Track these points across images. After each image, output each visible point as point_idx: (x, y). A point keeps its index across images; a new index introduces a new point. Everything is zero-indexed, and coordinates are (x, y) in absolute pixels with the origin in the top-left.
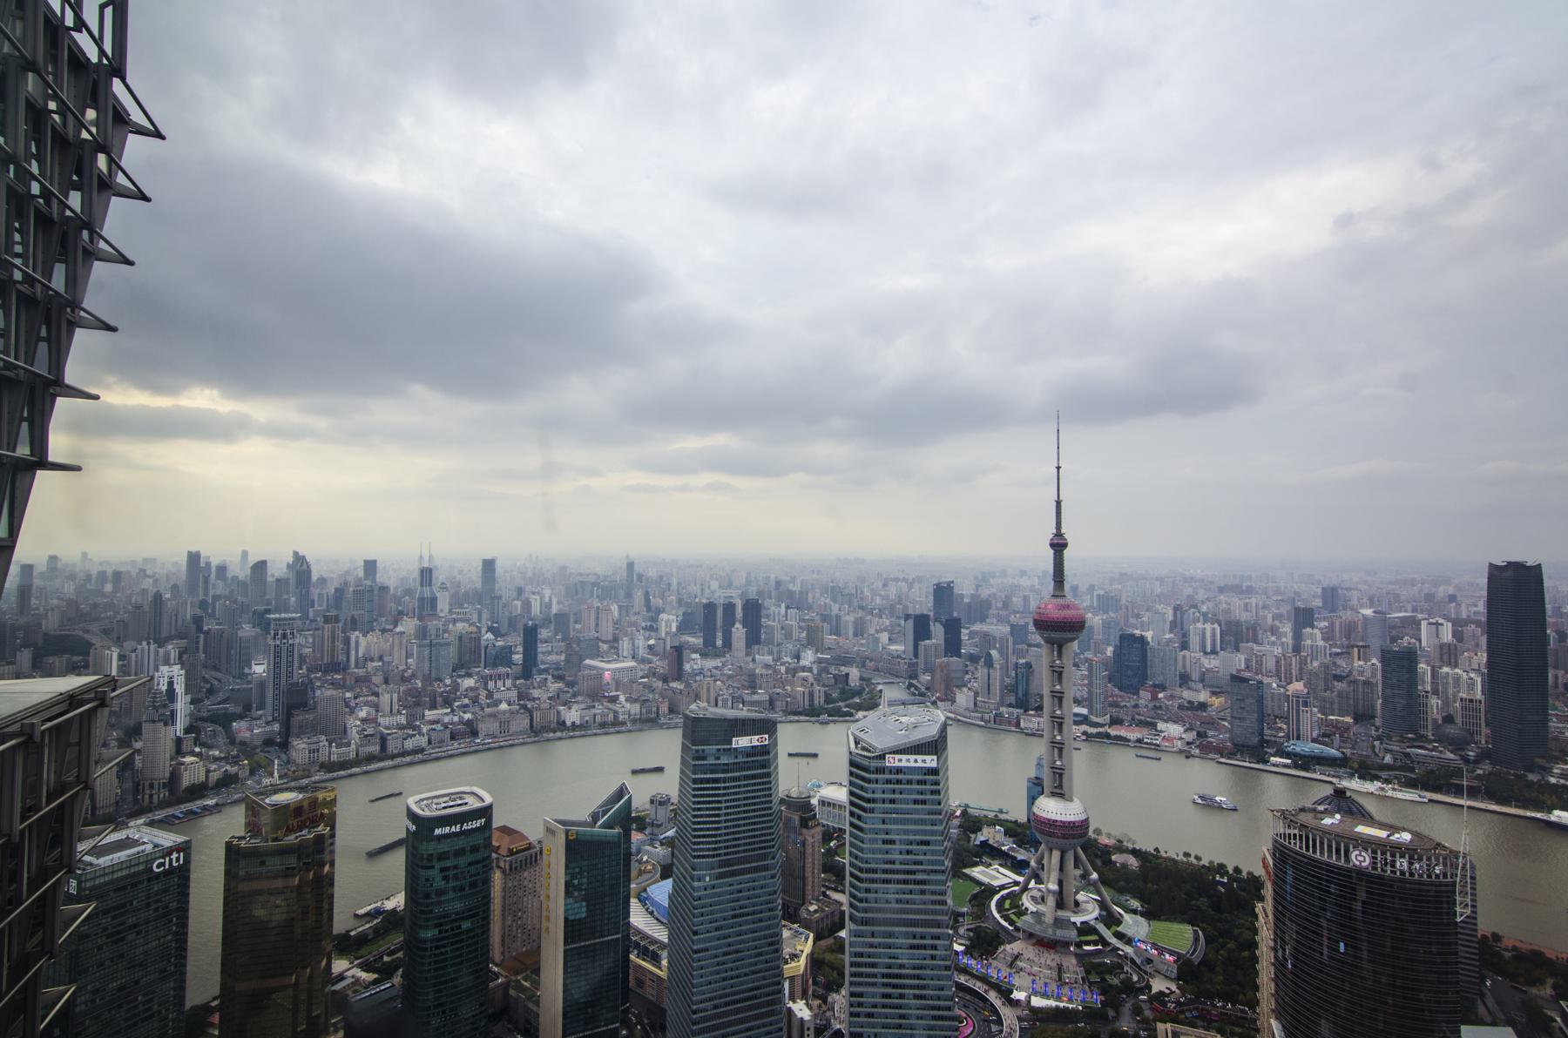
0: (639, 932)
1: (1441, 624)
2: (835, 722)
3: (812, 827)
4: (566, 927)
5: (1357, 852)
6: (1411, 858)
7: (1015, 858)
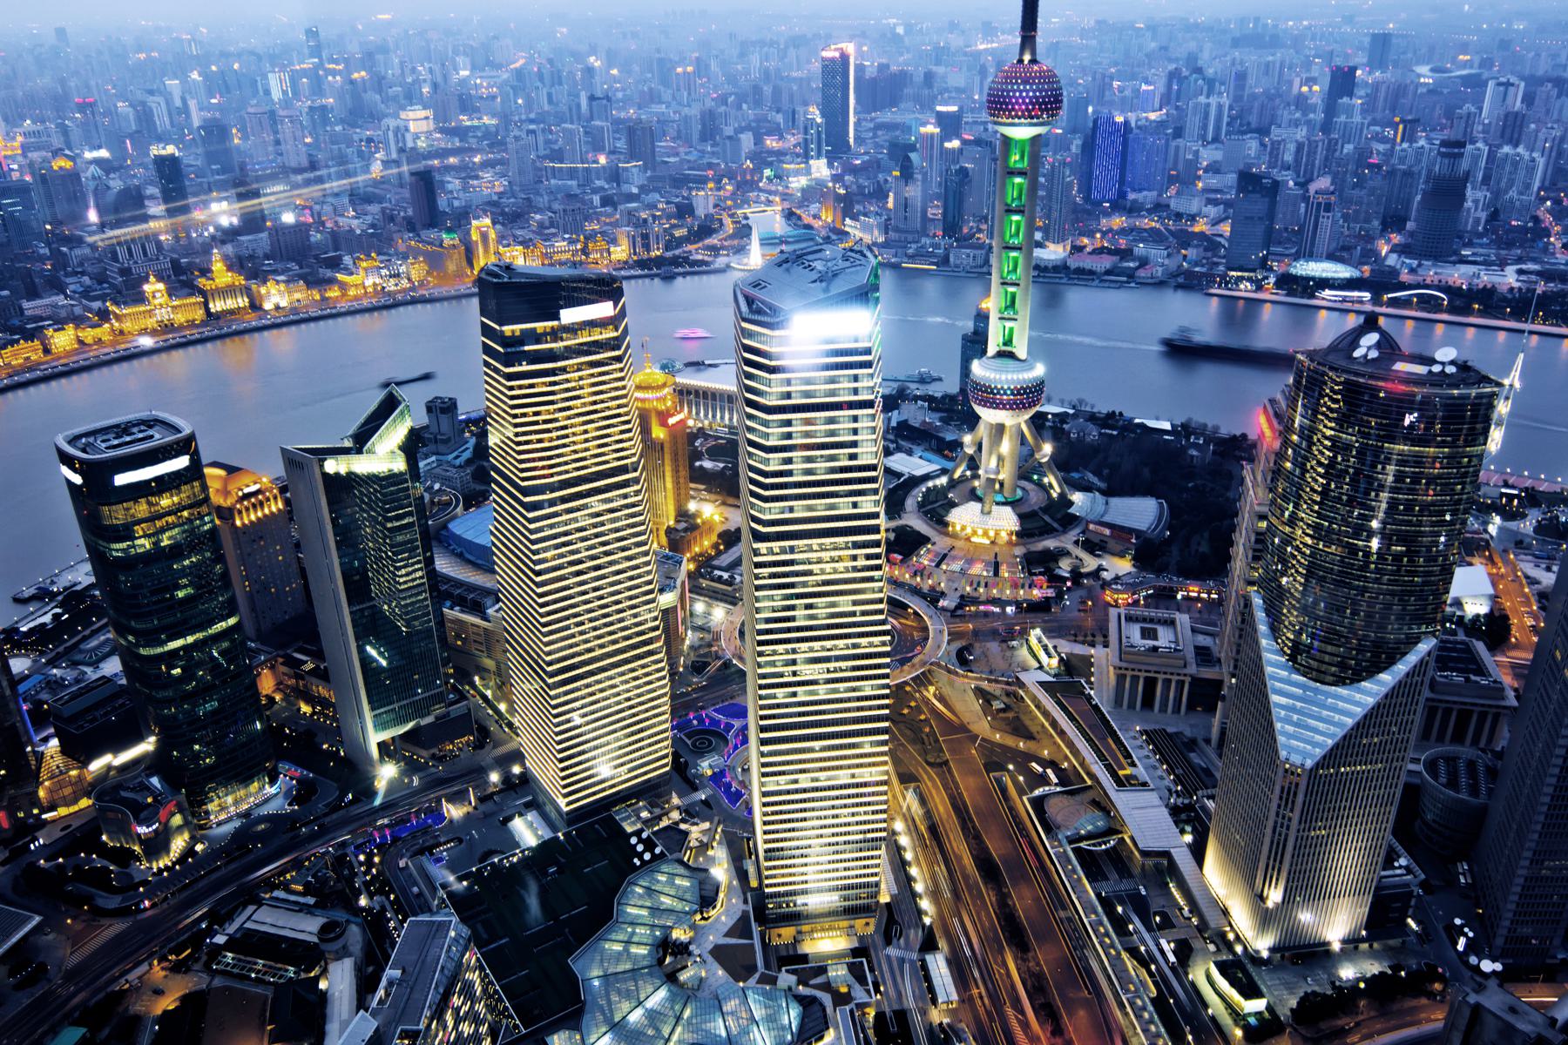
0: (448, 579)
1: (1512, 85)
2: (684, 275)
7: (943, 440)
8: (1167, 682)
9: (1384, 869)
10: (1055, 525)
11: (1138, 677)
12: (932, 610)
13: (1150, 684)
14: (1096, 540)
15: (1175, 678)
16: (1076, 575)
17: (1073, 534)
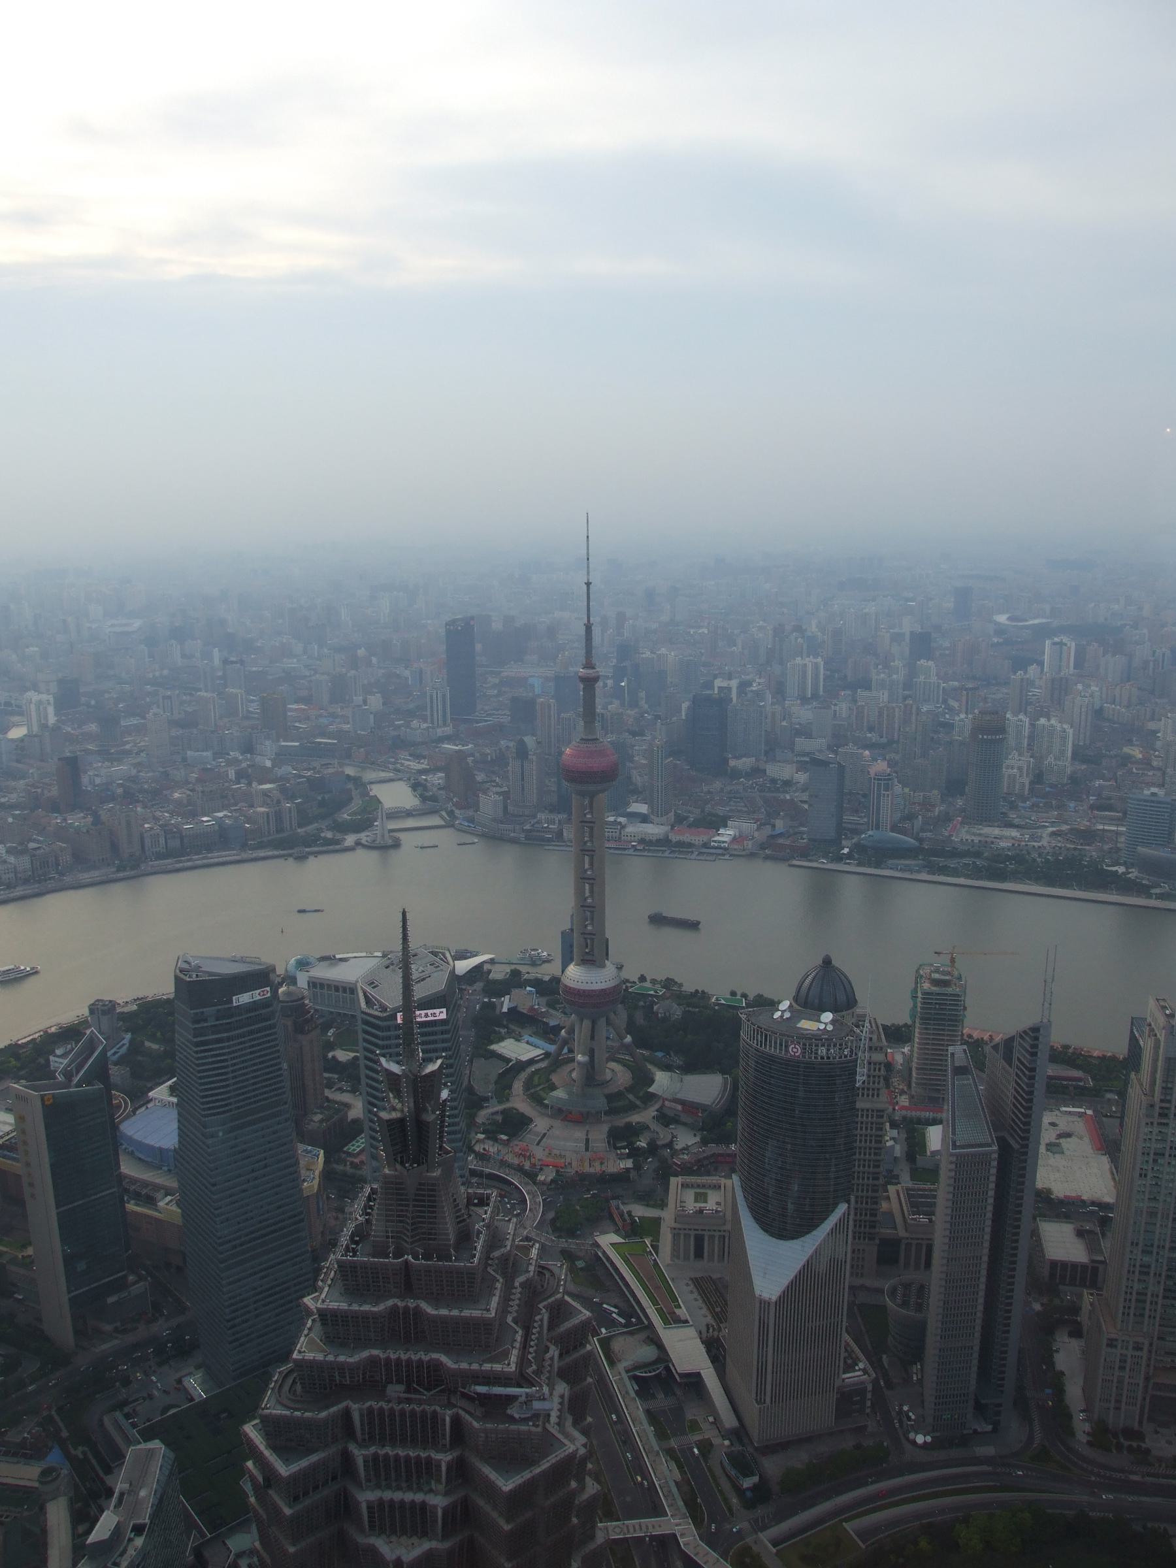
5: (793, 1046)
6: (829, 1045)
7: (546, 1024)
8: (712, 1237)
9: (844, 1373)
10: (638, 1103)
11: (690, 1235)
13: (699, 1240)
14: (671, 1114)
15: (717, 1234)
16: (653, 1148)
17: (652, 1112)
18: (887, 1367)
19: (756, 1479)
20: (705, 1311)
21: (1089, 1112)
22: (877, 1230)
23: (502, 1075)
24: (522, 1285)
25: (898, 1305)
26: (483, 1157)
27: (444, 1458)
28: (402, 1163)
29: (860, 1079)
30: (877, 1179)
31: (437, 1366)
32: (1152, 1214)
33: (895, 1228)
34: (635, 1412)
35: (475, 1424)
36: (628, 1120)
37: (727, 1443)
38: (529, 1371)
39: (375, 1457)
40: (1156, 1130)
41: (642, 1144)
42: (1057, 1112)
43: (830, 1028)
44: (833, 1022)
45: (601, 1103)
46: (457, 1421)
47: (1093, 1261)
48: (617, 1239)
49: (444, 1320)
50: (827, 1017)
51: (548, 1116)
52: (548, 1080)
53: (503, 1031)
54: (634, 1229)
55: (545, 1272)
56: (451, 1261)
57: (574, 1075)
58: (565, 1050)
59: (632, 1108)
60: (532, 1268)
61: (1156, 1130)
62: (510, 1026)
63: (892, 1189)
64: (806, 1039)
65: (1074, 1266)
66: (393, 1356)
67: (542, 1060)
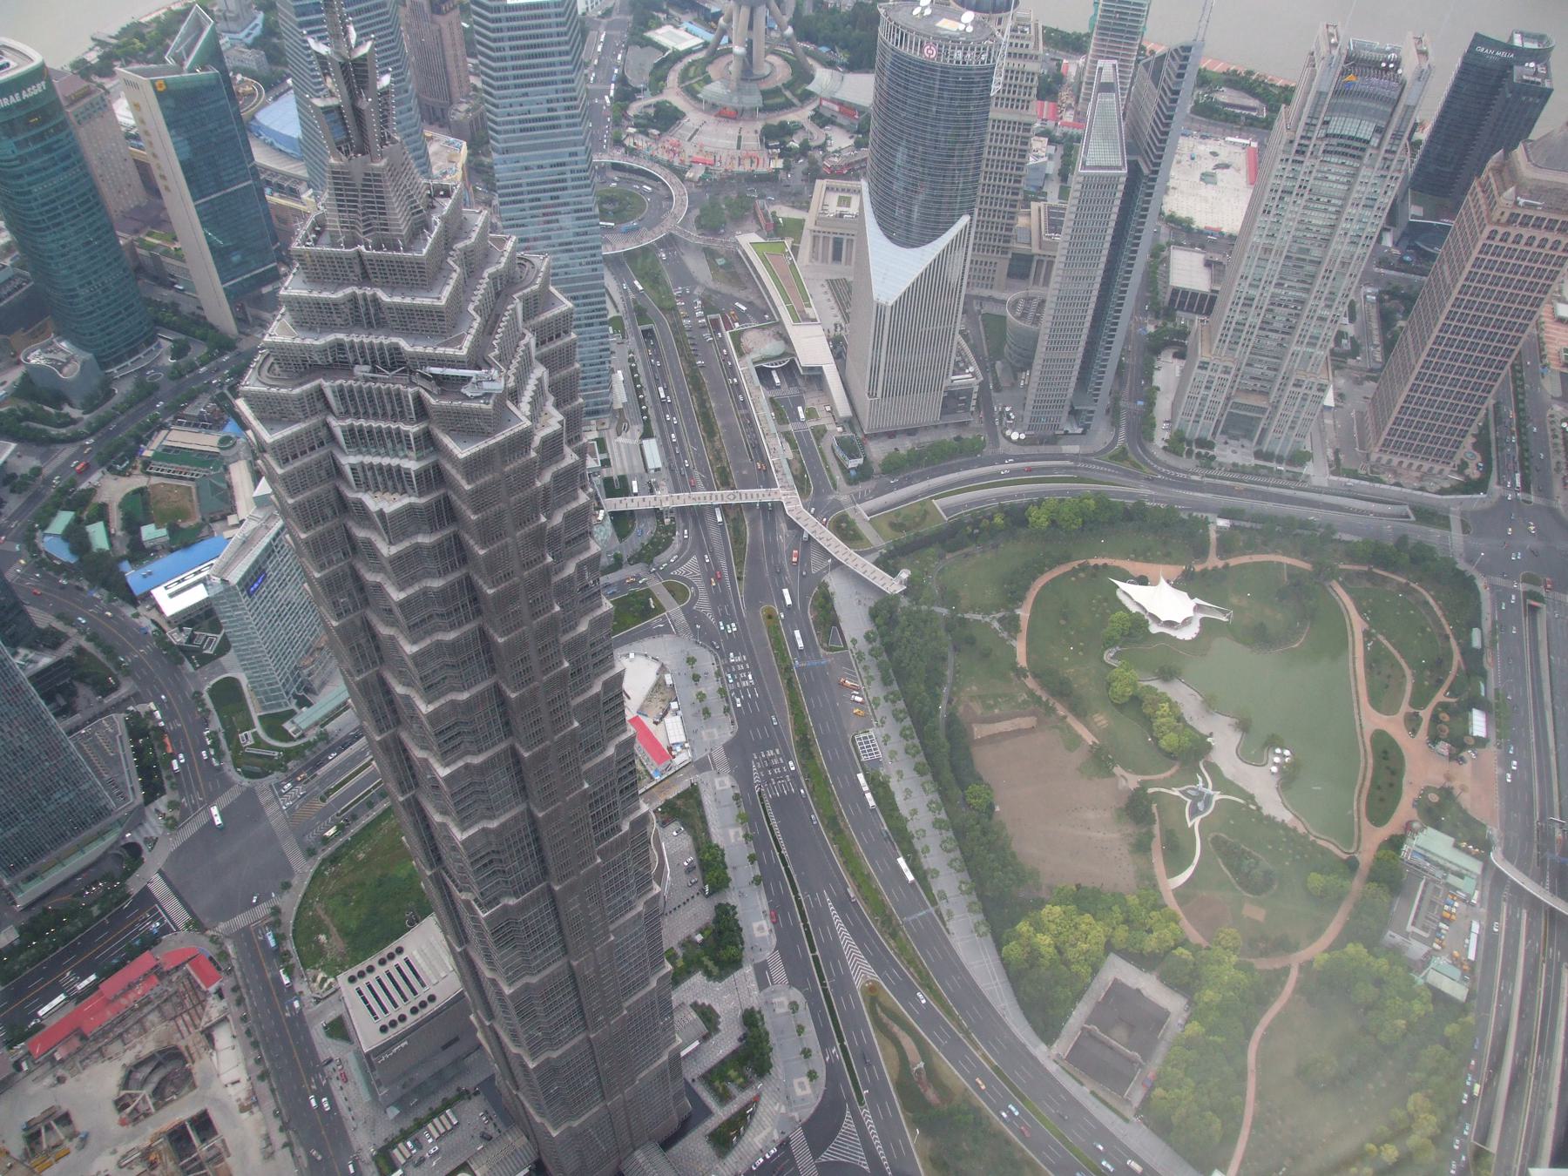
0: (266, 169)
3: (447, 12)
4: (185, 173)
10: (795, 101)
12: (676, 180)
13: (838, 244)
14: (828, 114)
16: (805, 148)
17: (808, 111)
18: (998, 372)
19: (860, 461)
20: (836, 311)
21: (1254, 145)
22: (1010, 245)
23: (658, 66)
24: (493, 277)
25: (1018, 318)
26: (632, 152)
27: (412, 429)
28: (347, 153)
29: (995, 88)
30: (1017, 194)
31: (396, 349)
32: (1267, 250)
33: (1030, 244)
34: (758, 399)
35: (433, 401)
36: (783, 118)
37: (840, 429)
38: (491, 355)
39: (351, 429)
40: (1289, 167)
41: (795, 143)
42: (1222, 142)
43: (970, 29)
44: (975, 23)
45: (756, 100)
46: (419, 399)
47: (1212, 291)
48: (757, 239)
49: (399, 309)
50: (968, 16)
51: (701, 110)
52: (704, 72)
53: (662, 16)
54: (777, 230)
55: (527, 264)
56: (398, 250)
57: (731, 68)
58: (725, 40)
59: (788, 105)
60: (504, 260)
61: (1289, 167)
62: (672, 12)
63: (1034, 205)
64: (943, 40)
65: (1194, 294)
66: (356, 340)
67: (700, 50)
